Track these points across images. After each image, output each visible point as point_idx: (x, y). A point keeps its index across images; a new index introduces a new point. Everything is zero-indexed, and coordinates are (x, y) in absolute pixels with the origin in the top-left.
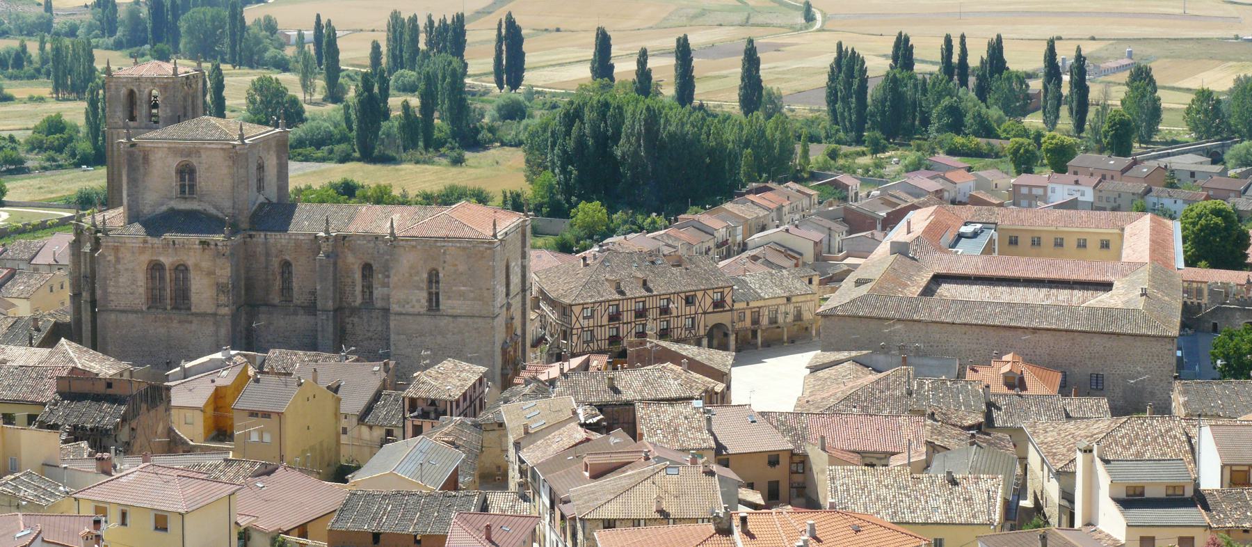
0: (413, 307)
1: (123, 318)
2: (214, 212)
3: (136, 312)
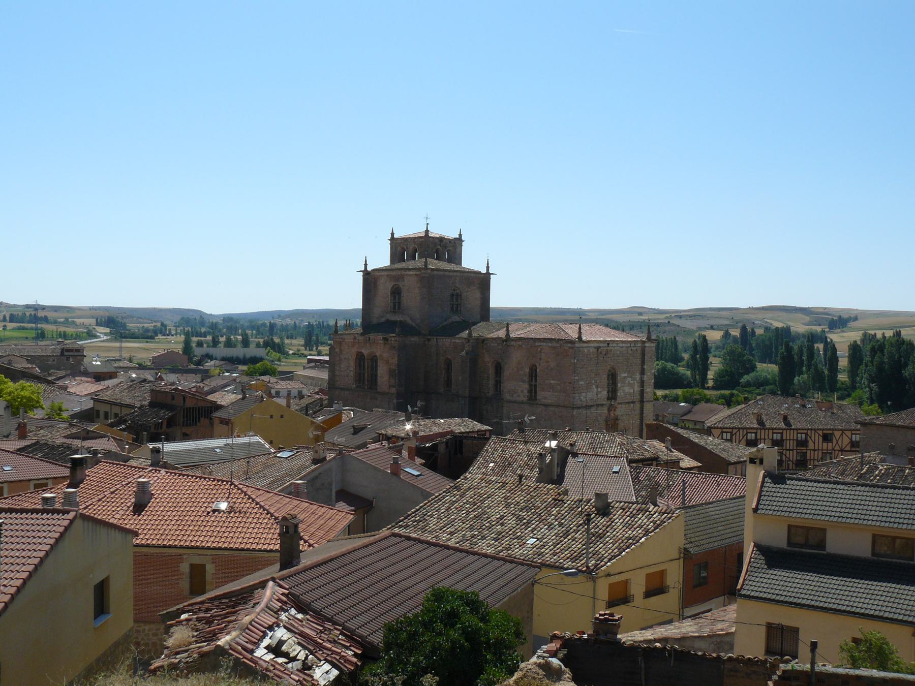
0: (519, 396)
3: (348, 390)
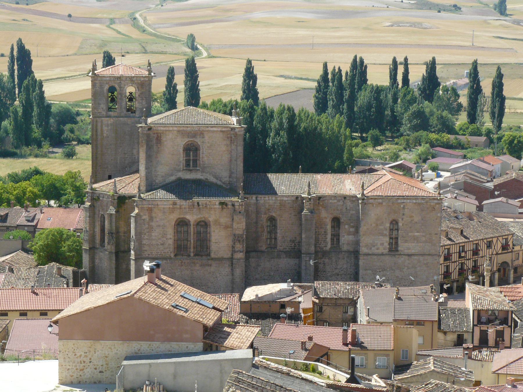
2: (214, 180)
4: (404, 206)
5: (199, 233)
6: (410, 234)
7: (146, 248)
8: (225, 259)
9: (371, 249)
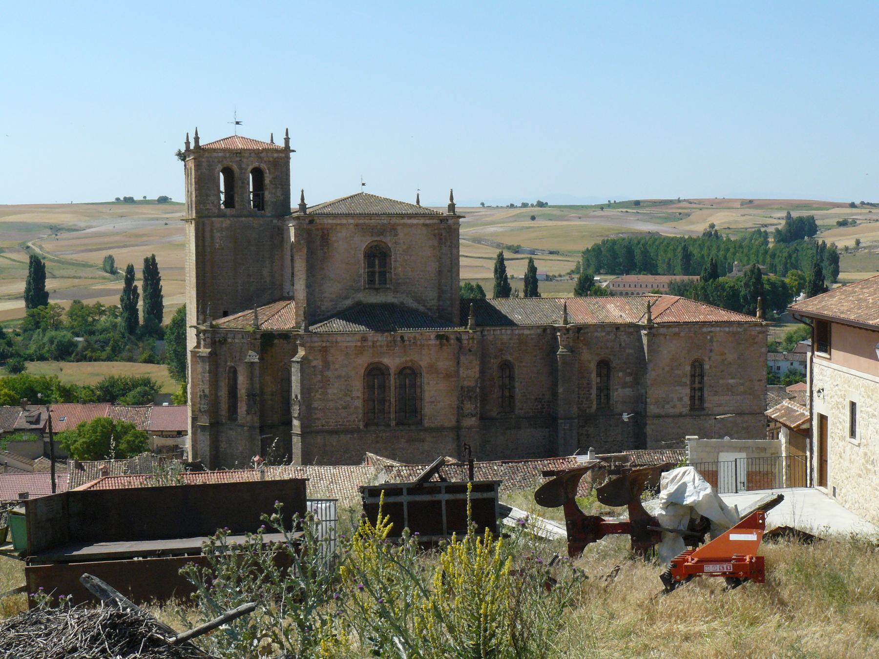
0: (674, 407)
1: (334, 440)
2: (414, 305)
3: (351, 431)
4: (712, 337)
5: (402, 387)
6: (721, 382)
7: (319, 414)
8: (448, 428)
9: (663, 407)
